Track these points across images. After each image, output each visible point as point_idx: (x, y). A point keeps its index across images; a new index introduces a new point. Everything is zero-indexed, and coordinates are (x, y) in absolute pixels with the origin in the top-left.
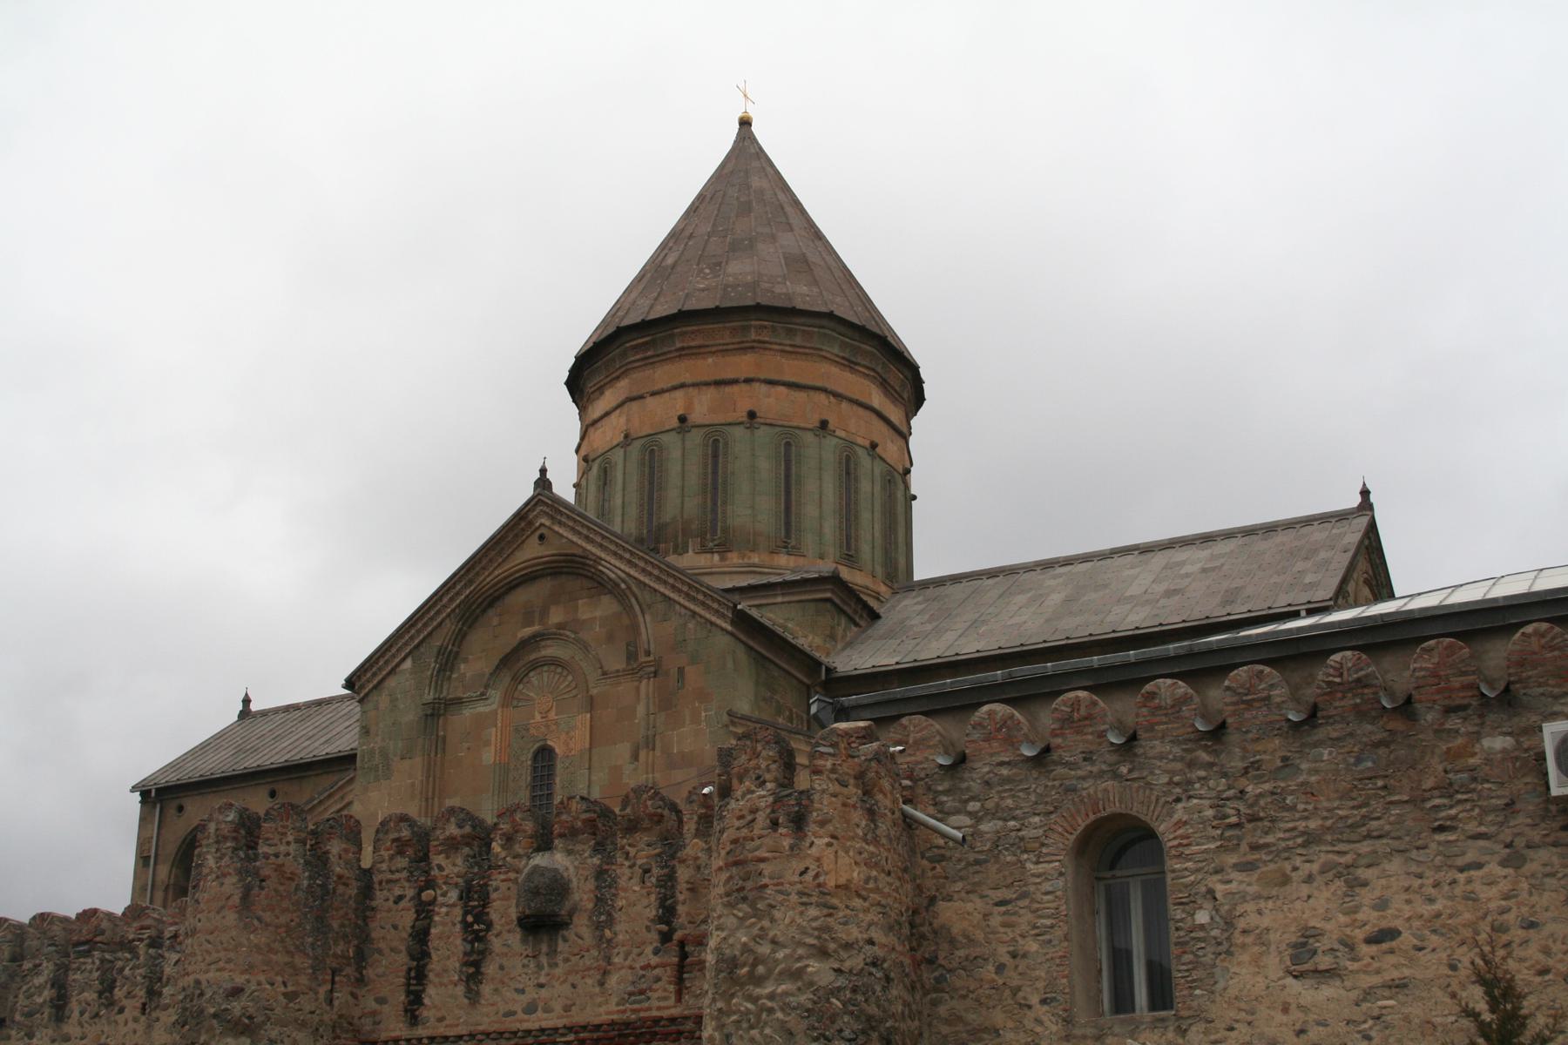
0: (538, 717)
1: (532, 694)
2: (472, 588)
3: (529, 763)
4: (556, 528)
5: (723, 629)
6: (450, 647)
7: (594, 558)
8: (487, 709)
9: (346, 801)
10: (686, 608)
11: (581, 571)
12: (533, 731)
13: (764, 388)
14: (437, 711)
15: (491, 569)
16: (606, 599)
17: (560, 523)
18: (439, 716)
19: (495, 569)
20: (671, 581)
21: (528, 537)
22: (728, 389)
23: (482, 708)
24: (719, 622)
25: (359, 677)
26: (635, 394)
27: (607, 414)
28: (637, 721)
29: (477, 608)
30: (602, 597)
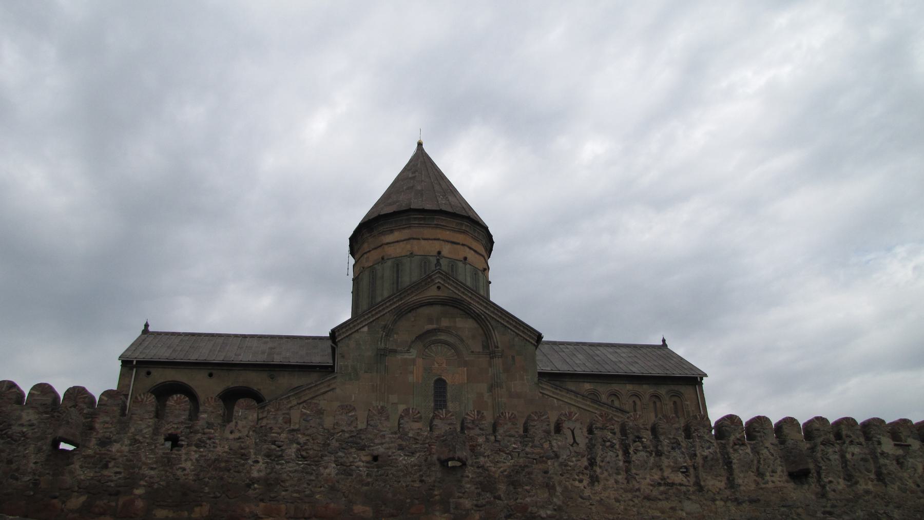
0: (436, 365)
2: (403, 302)
3: (433, 385)
4: (447, 285)
5: (532, 343)
6: (390, 326)
8: (410, 357)
9: (331, 388)
10: (513, 331)
14: (382, 354)
15: (413, 296)
17: (448, 283)
18: (386, 356)
21: (431, 286)
23: (406, 356)
24: (531, 340)
26: (415, 237)
27: (398, 242)
29: (404, 311)
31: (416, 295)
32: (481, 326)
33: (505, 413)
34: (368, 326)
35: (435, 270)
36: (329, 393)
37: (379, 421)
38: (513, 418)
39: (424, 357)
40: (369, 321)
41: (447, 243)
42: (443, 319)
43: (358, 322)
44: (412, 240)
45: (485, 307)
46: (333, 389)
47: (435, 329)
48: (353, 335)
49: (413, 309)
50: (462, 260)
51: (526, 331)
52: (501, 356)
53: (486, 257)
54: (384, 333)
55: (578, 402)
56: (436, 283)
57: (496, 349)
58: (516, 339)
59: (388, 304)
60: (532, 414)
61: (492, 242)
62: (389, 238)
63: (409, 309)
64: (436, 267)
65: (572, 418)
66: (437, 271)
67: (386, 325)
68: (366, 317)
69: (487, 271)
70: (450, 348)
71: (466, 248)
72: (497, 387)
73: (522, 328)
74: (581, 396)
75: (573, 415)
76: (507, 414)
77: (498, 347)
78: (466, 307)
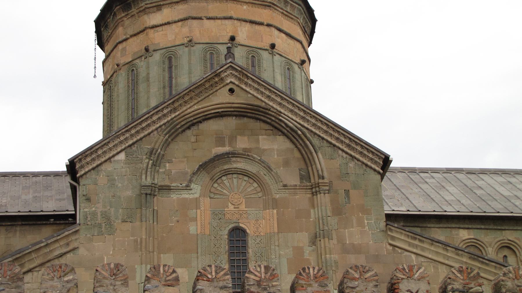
0: (231, 207)
1: (225, 191)
2: (177, 113)
3: (227, 237)
4: (243, 86)
5: (375, 170)
6: (159, 150)
7: (275, 111)
8: (191, 196)
9: (71, 247)
10: (347, 153)
11: (262, 118)
12: (228, 216)
13: (276, 32)
15: (192, 104)
16: (281, 139)
17: (246, 84)
18: (155, 195)
19: (194, 105)
20: (336, 135)
22: (257, 27)
23: (185, 195)
24: (373, 166)
25: (80, 160)
27: (168, 23)
28: (311, 220)
29: (180, 128)
30: (278, 137)
31: (197, 103)
32: (296, 147)
33: (309, 268)
34: (126, 152)
35: (226, 65)
36: (68, 255)
37: (112, 287)
38: (321, 276)
39: (212, 195)
40: (127, 145)
41: (244, 23)
42: (239, 137)
43: (111, 145)
44: (190, 22)
45: (303, 118)
46: (74, 249)
47: (227, 154)
48: (103, 167)
49: (193, 125)
50: (268, 48)
51: (365, 152)
52: (329, 190)
53: (305, 43)
54: (151, 162)
55: (448, 258)
56: (227, 84)
57: (321, 181)
58: (351, 165)
59: (155, 118)
60: (350, 270)
61: (313, 21)
62: (156, 18)
63: (188, 124)
64: (226, 60)
65: (414, 275)
66: (228, 65)
67: (153, 149)
68: (122, 138)
69: (306, 64)
70: (251, 181)
71: (273, 29)
72: (324, 238)
73: (359, 148)
74: (454, 250)
75: (415, 271)
76: (311, 270)
77: (323, 178)
78: (273, 119)
